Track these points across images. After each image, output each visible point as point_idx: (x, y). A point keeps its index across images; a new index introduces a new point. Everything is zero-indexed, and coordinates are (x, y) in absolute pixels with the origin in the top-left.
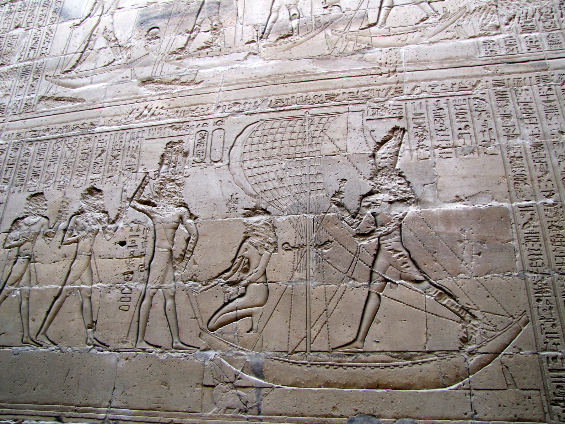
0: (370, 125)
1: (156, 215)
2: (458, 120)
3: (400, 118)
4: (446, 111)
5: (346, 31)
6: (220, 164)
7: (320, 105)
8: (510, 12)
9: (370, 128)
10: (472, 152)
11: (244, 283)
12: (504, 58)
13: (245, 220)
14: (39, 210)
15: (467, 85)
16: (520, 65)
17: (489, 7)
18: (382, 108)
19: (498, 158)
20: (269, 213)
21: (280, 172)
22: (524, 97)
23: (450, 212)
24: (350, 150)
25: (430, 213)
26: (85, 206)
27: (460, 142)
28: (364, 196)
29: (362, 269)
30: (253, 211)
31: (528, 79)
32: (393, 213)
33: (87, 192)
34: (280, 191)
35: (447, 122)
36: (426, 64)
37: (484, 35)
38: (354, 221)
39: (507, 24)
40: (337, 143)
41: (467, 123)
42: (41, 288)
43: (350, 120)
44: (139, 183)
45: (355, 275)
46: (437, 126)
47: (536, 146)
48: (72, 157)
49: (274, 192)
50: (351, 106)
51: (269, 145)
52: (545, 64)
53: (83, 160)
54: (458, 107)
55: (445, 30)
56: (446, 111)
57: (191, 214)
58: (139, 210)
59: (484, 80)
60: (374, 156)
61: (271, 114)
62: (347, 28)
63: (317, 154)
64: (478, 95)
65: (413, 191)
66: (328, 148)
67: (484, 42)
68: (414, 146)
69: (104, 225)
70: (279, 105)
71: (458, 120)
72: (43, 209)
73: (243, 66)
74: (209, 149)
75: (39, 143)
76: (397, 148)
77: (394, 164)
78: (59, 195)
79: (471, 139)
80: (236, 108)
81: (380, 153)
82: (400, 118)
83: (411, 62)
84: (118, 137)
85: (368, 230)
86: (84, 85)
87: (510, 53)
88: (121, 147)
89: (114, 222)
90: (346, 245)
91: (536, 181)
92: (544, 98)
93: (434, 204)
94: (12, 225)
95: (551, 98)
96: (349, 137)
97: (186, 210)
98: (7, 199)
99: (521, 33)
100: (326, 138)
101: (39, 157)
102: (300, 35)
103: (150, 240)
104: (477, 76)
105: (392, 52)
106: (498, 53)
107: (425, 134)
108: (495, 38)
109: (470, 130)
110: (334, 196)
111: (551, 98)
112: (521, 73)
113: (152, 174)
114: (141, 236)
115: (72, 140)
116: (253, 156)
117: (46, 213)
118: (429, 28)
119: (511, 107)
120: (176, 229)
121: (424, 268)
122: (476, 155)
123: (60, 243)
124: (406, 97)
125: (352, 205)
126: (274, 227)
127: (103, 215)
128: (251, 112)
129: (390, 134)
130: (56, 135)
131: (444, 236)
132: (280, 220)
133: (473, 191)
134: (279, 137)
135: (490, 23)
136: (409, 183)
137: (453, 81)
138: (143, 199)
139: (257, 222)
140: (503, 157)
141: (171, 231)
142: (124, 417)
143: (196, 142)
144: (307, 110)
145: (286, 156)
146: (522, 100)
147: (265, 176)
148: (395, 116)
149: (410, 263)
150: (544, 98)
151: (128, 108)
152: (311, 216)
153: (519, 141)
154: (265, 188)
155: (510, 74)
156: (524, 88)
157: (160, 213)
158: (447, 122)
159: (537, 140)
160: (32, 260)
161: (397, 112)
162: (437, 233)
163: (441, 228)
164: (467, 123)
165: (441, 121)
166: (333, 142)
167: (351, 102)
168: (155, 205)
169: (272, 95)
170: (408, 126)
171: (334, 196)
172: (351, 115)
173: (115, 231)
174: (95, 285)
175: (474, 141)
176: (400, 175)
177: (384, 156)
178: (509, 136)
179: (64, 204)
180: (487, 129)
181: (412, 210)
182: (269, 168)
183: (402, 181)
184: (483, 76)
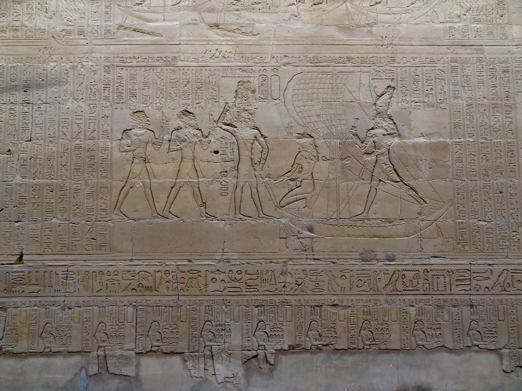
0: (374, 83)
1: (237, 134)
2: (427, 84)
3: (393, 79)
4: (420, 78)
5: (360, 6)
6: (278, 101)
7: (342, 64)
8: (468, 5)
9: (374, 85)
10: (433, 106)
11: (299, 179)
13: (298, 141)
14: (143, 124)
15: (435, 60)
18: (382, 71)
19: (447, 111)
20: (312, 137)
21: (318, 111)
22: (467, 72)
23: (417, 143)
24: (361, 99)
25: (406, 143)
26: (182, 124)
27: (426, 99)
28: (369, 130)
29: (367, 175)
30: (302, 135)
31: (471, 59)
32: (385, 142)
33: (181, 114)
34: (319, 123)
35: (420, 85)
36: (411, 41)
37: (449, 22)
38: (363, 145)
39: (465, 15)
40: (353, 93)
41: (431, 87)
42: (159, 181)
43: (362, 79)
44: (222, 110)
45: (363, 177)
46: (414, 87)
47: (469, 105)
48: (162, 84)
49: (315, 124)
50: (362, 68)
51: (310, 91)
52: (482, 49)
53: (173, 88)
54: (428, 75)
55: (426, 15)
56: (420, 78)
57: (262, 135)
58: (224, 130)
59: (445, 56)
60: (375, 104)
61: (310, 68)
62: (361, 4)
63: (341, 100)
64: (440, 68)
65: (397, 129)
66: (348, 97)
67: (450, 27)
68: (400, 100)
69: (200, 139)
70: (316, 62)
71: (427, 84)
72: (147, 124)
73: (288, 25)
74: (269, 90)
75: (129, 69)
76: (389, 100)
77: (387, 111)
78: (158, 114)
79: (433, 98)
80: (285, 60)
81: (378, 102)
82: (393, 79)
83: (402, 38)
84: (199, 72)
85: (370, 151)
86: (157, 21)
87: (464, 38)
88: (203, 81)
89: (207, 137)
90: (358, 160)
91: (466, 126)
93: (409, 138)
94: (122, 134)
95: (482, 74)
96: (361, 90)
97: (258, 132)
98: (112, 114)
99: (473, 23)
100: (346, 90)
101: (132, 81)
102: (328, 4)
103: (236, 151)
105: (390, 29)
107: (407, 92)
108: (456, 26)
109: (433, 92)
110: (351, 129)
111: (482, 74)
112: (468, 54)
113: (231, 104)
114: (229, 148)
115: (159, 70)
116: (300, 98)
117: (151, 127)
118: (415, 11)
119: (459, 78)
120: (253, 144)
121: (401, 174)
122: (435, 108)
123: (167, 150)
124: (396, 65)
125: (362, 135)
126: (316, 146)
127: (197, 131)
128: (297, 64)
129: (386, 91)
130: (144, 64)
131: (413, 157)
132: (319, 142)
133: (431, 131)
134: (316, 85)
135: (455, 12)
136: (395, 123)
137: (427, 56)
138: (226, 122)
139: (305, 142)
140: (450, 111)
141: (250, 145)
142: (233, 257)
143: (260, 84)
144: (334, 67)
145: (322, 100)
146: (465, 74)
147: (309, 112)
148: (389, 78)
149: (393, 171)
150: (478, 74)
151: (201, 49)
152: (338, 141)
154: (309, 121)
155: (461, 54)
156: (468, 65)
157: (240, 132)
158: (420, 85)
159: (470, 101)
160: (147, 161)
161: (391, 75)
162: (409, 155)
163: (412, 152)
164: (431, 87)
165: (417, 84)
166: (351, 93)
167: (362, 65)
168: (236, 127)
169: (311, 53)
170: (397, 85)
171: (351, 129)
172: (363, 75)
173: (209, 143)
174: (200, 180)
175: (435, 99)
176: (390, 118)
177: (381, 105)
179: (164, 121)
180: (443, 92)
181: (396, 140)
182: (311, 107)
183: (391, 122)
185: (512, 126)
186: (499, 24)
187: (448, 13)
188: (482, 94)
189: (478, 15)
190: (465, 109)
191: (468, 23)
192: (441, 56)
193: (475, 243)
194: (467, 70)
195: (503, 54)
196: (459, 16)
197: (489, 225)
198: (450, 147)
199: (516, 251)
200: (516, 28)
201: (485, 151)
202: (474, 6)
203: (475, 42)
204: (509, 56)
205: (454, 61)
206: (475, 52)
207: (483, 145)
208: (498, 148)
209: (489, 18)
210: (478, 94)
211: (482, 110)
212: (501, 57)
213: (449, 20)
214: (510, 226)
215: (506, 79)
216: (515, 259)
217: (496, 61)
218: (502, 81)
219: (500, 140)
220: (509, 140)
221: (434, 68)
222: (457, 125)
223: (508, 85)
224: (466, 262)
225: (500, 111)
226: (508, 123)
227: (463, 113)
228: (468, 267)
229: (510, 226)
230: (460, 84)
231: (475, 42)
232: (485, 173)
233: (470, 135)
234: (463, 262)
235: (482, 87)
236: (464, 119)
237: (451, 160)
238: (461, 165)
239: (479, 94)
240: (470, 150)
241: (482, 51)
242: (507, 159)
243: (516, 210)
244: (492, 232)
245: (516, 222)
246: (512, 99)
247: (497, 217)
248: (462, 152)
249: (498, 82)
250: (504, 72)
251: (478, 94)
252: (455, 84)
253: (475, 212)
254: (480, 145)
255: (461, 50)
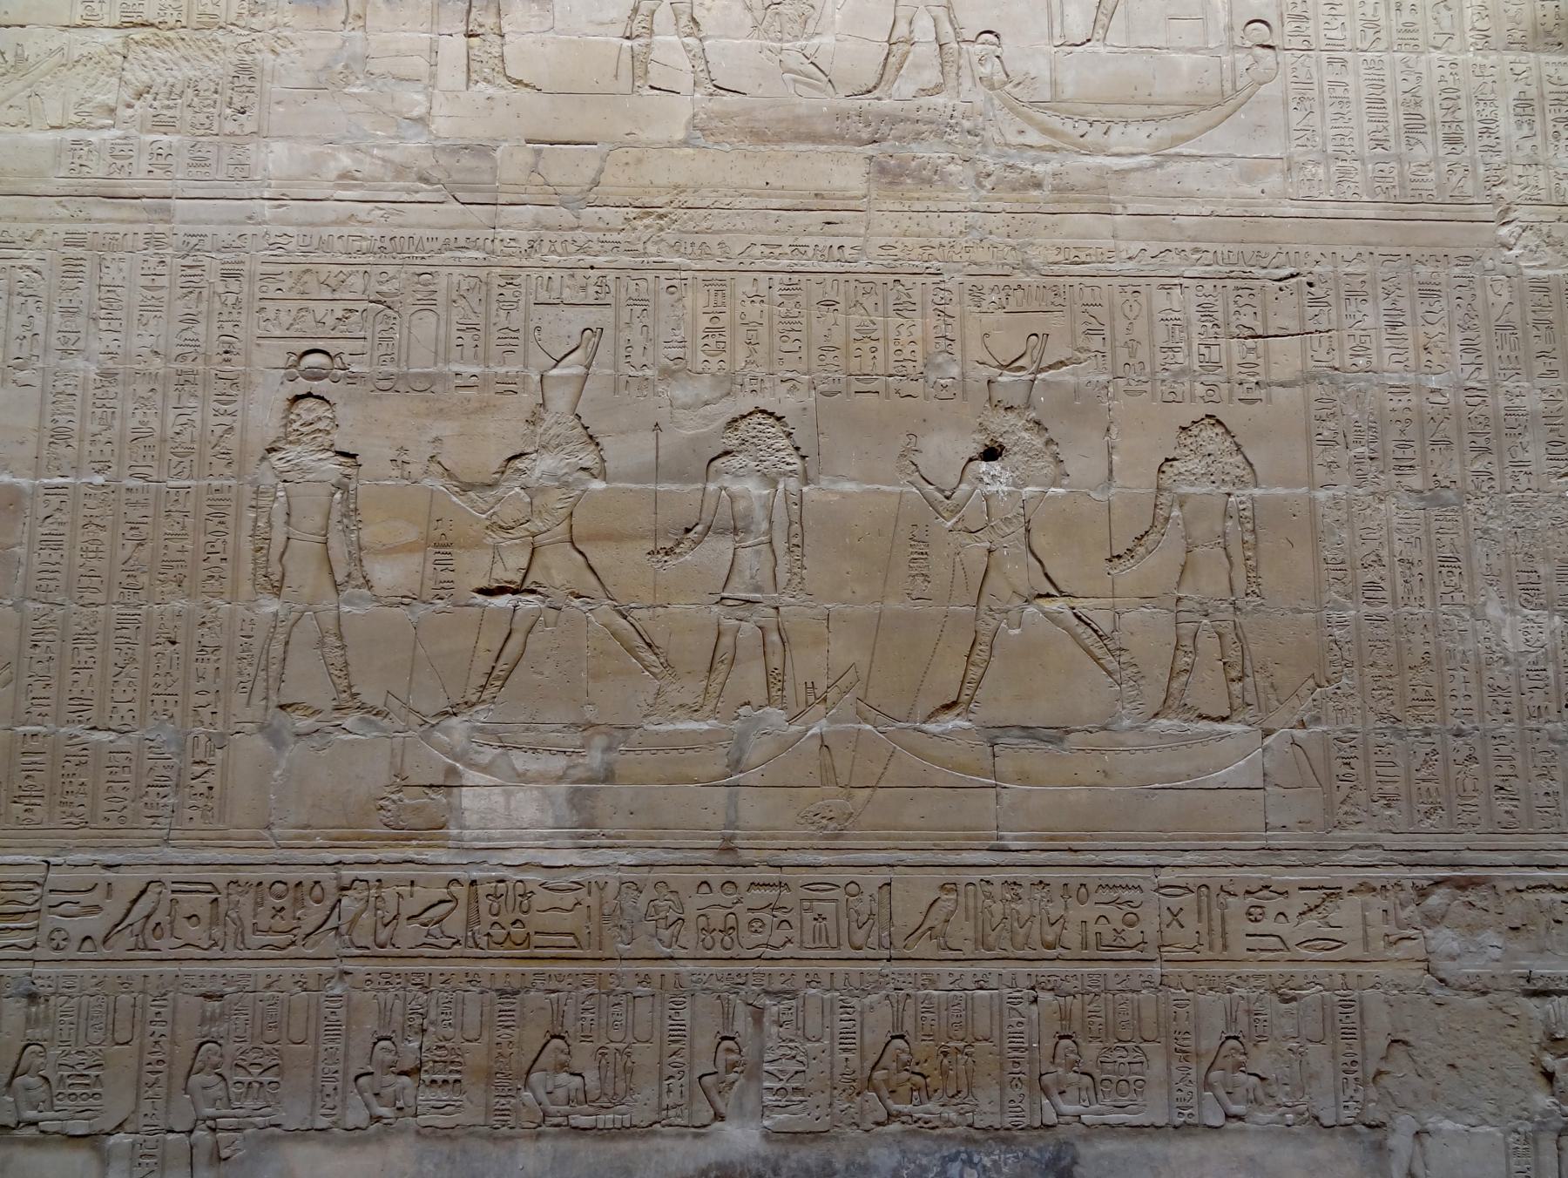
12: (100, 185)
15: (16, 238)
16: (124, 205)
17: (109, 58)
37: (78, 125)
39: (130, 106)
47: (108, 375)
52: (168, 209)
59: (49, 228)
67: (75, 142)
87: (115, 175)
91: (88, 438)
92: (146, 281)
95: (160, 281)
99: (150, 132)
104: (40, 220)
106: (94, 173)
108: (94, 137)
111: (160, 281)
112: (122, 221)
135: (100, 98)
140: (43, 391)
146: (106, 280)
150: (146, 281)
153: (80, 363)
155: (101, 221)
156: (116, 255)
159: (110, 364)
178: (65, 351)
180: (29, 334)
184: (52, 220)
185: (232, 442)
186: (233, 134)
187: (75, 98)
188: (149, 341)
189: (169, 107)
190: (91, 386)
191: (133, 132)
192: (35, 226)
193: (70, 798)
194: (113, 271)
195: (230, 222)
196: (112, 111)
197: (123, 743)
198: (28, 503)
199: (198, 823)
200: (279, 147)
201: (135, 515)
202: (160, 80)
203: (147, 186)
204: (249, 229)
205: (74, 241)
206: (144, 216)
207: (133, 497)
208: (179, 507)
209: (202, 118)
210: (137, 341)
211: (142, 389)
212: (224, 233)
213: (77, 119)
214: (189, 744)
215: (231, 299)
216: (192, 847)
217: (207, 245)
218: (217, 306)
219: (187, 483)
220: (216, 483)
221: (10, 263)
222: (60, 436)
223: (235, 316)
224: (32, 859)
225: (200, 393)
226: (219, 430)
227: (83, 401)
228: (34, 874)
229: (189, 744)
230: (85, 311)
231: (147, 186)
232: (125, 581)
233: (97, 466)
234: (21, 859)
235: (153, 322)
236: (83, 416)
237: (25, 540)
238: (55, 557)
239: (141, 341)
240: (88, 512)
241: (167, 215)
242: (203, 539)
243: (211, 697)
244: (126, 763)
245: (209, 735)
246: (241, 358)
247: (150, 720)
248: (65, 519)
249: (203, 307)
250: (226, 276)
251: (137, 341)
252: (69, 312)
253: (81, 705)
254: (125, 495)
255: (100, 211)
